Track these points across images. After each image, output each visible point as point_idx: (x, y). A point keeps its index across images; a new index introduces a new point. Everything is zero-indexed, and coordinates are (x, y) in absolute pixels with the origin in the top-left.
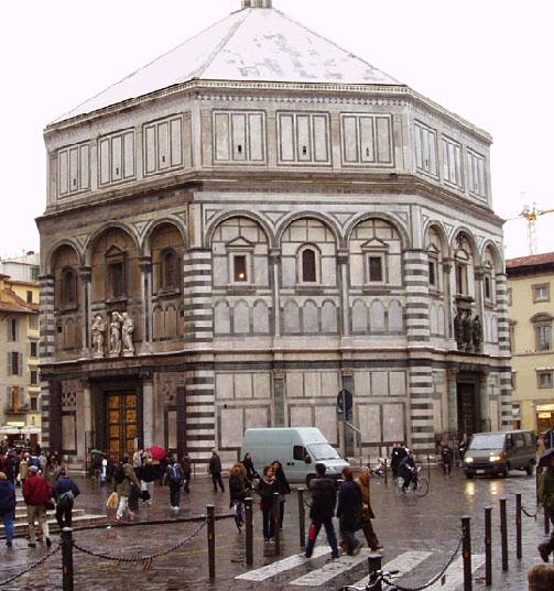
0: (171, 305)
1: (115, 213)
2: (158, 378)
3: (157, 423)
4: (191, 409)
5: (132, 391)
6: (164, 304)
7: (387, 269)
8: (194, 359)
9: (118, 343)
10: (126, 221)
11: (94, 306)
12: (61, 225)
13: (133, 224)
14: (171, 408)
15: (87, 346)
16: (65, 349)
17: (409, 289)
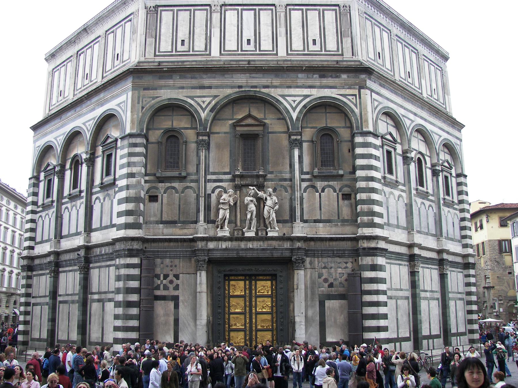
0: (330, 186)
1: (254, 82)
2: (311, 263)
3: (310, 313)
4: (367, 298)
5: (273, 277)
6: (319, 184)
7: (452, 187)
8: (373, 245)
9: (254, 222)
10: (275, 93)
11: (214, 177)
12: (171, 82)
13: (283, 96)
14: (330, 297)
15: (205, 222)
16: (162, 222)
17: (461, 206)
